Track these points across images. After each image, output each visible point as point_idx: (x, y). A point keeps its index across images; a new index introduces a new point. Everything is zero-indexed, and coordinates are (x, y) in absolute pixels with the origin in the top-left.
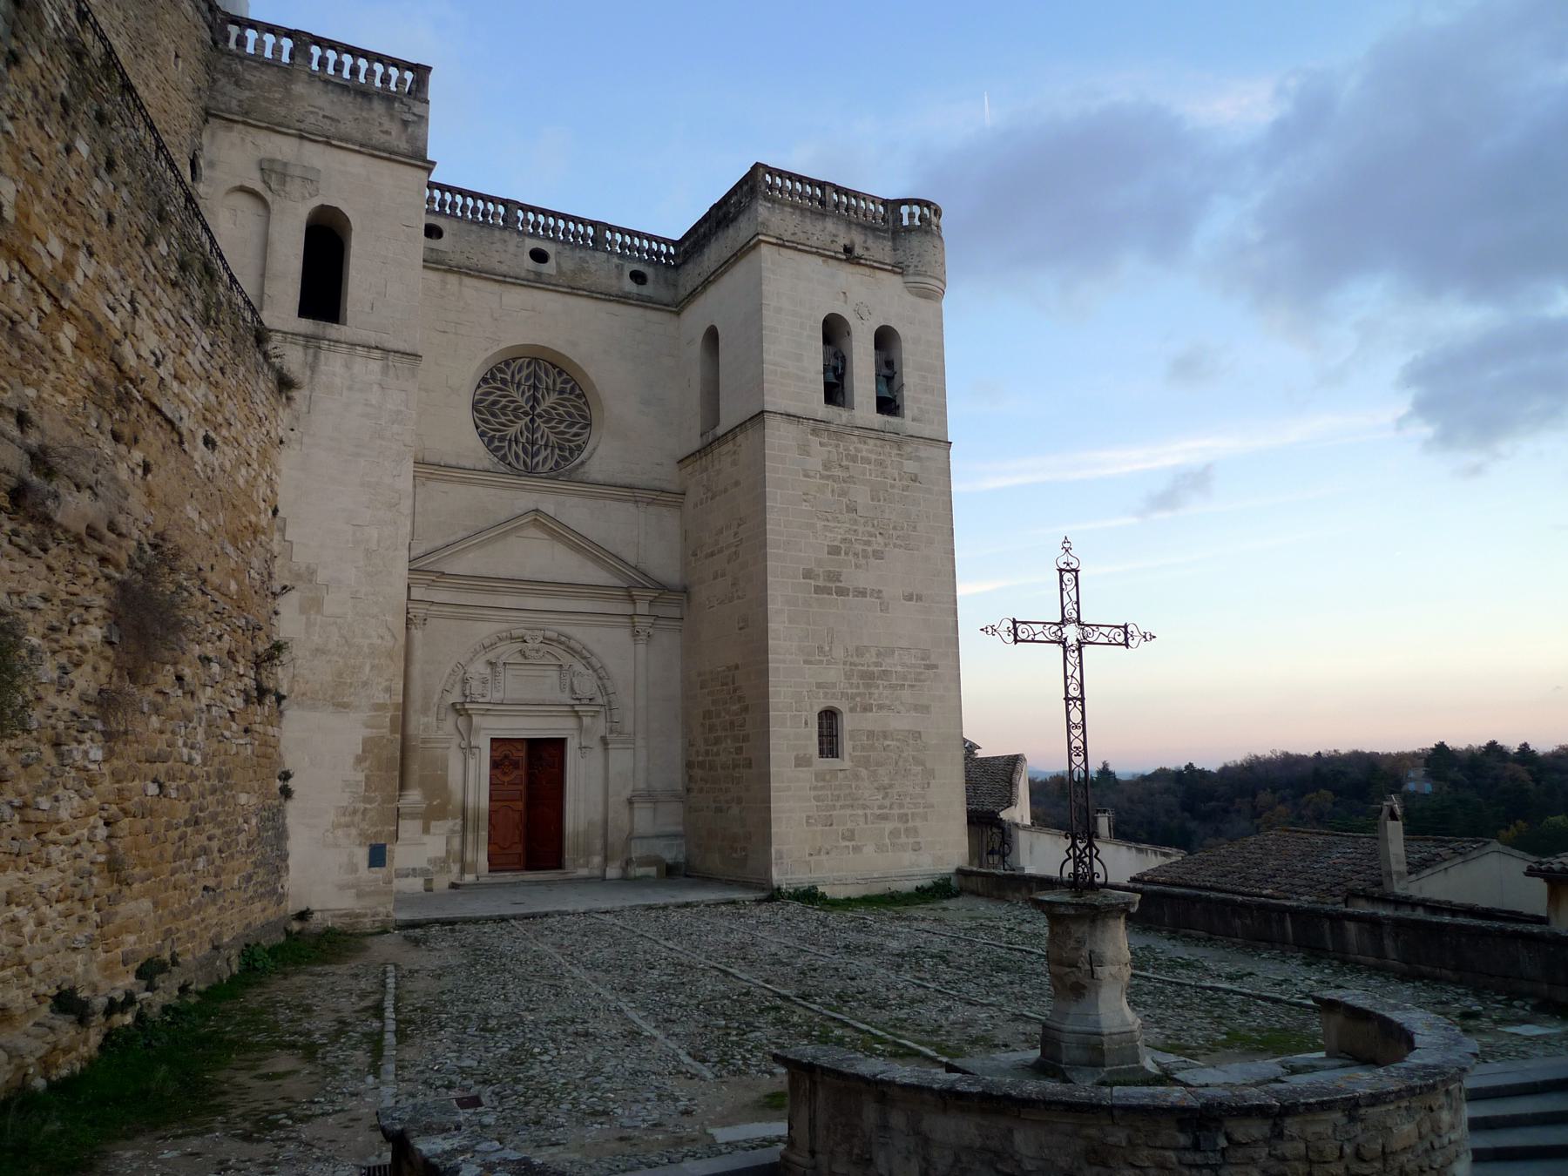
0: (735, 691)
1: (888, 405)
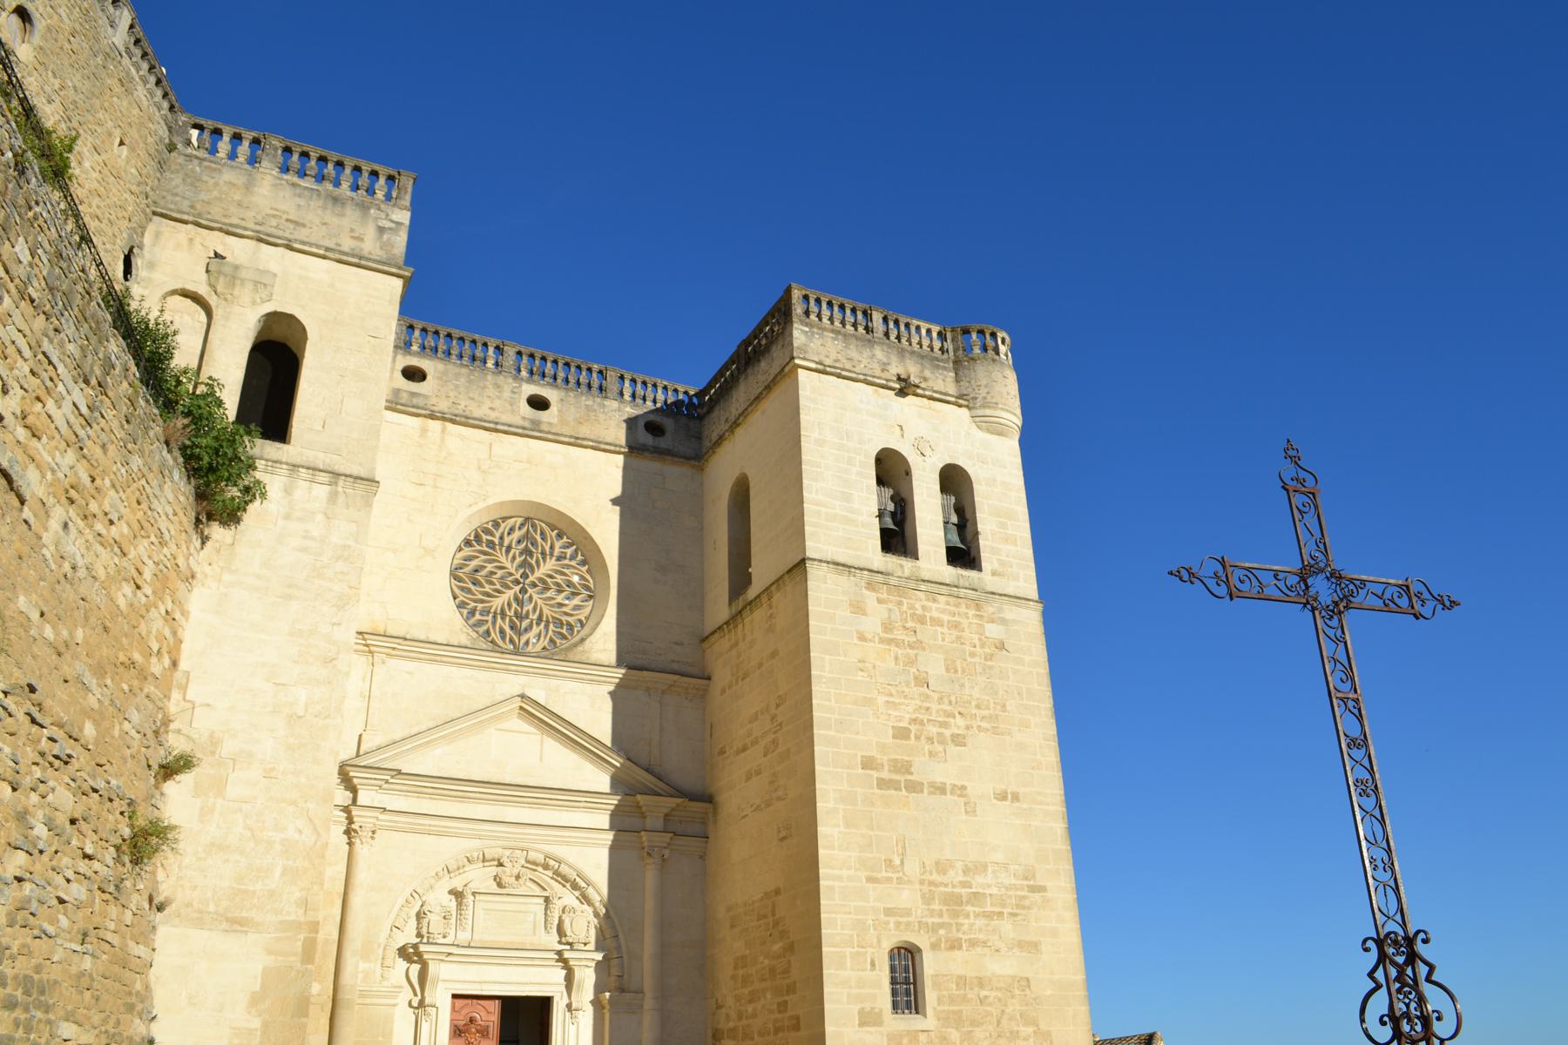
0: (776, 924)
1: (963, 555)
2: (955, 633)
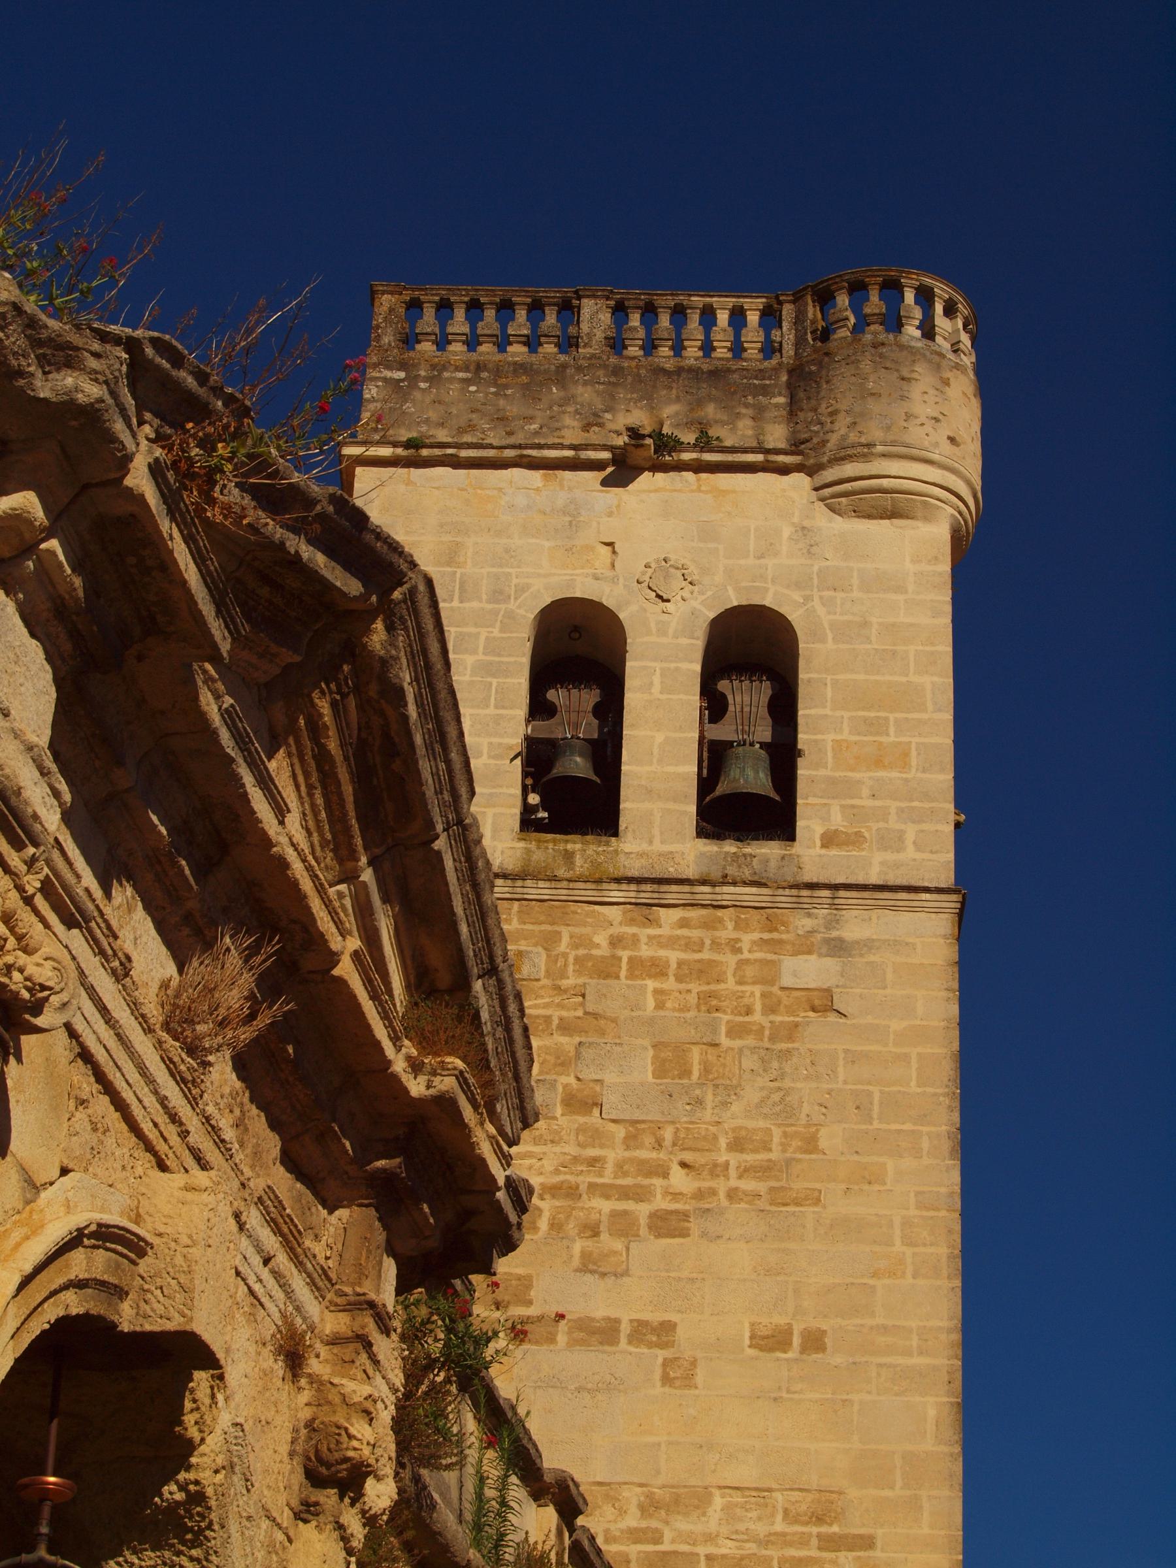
2: (696, 987)
